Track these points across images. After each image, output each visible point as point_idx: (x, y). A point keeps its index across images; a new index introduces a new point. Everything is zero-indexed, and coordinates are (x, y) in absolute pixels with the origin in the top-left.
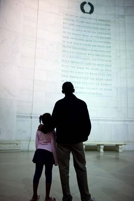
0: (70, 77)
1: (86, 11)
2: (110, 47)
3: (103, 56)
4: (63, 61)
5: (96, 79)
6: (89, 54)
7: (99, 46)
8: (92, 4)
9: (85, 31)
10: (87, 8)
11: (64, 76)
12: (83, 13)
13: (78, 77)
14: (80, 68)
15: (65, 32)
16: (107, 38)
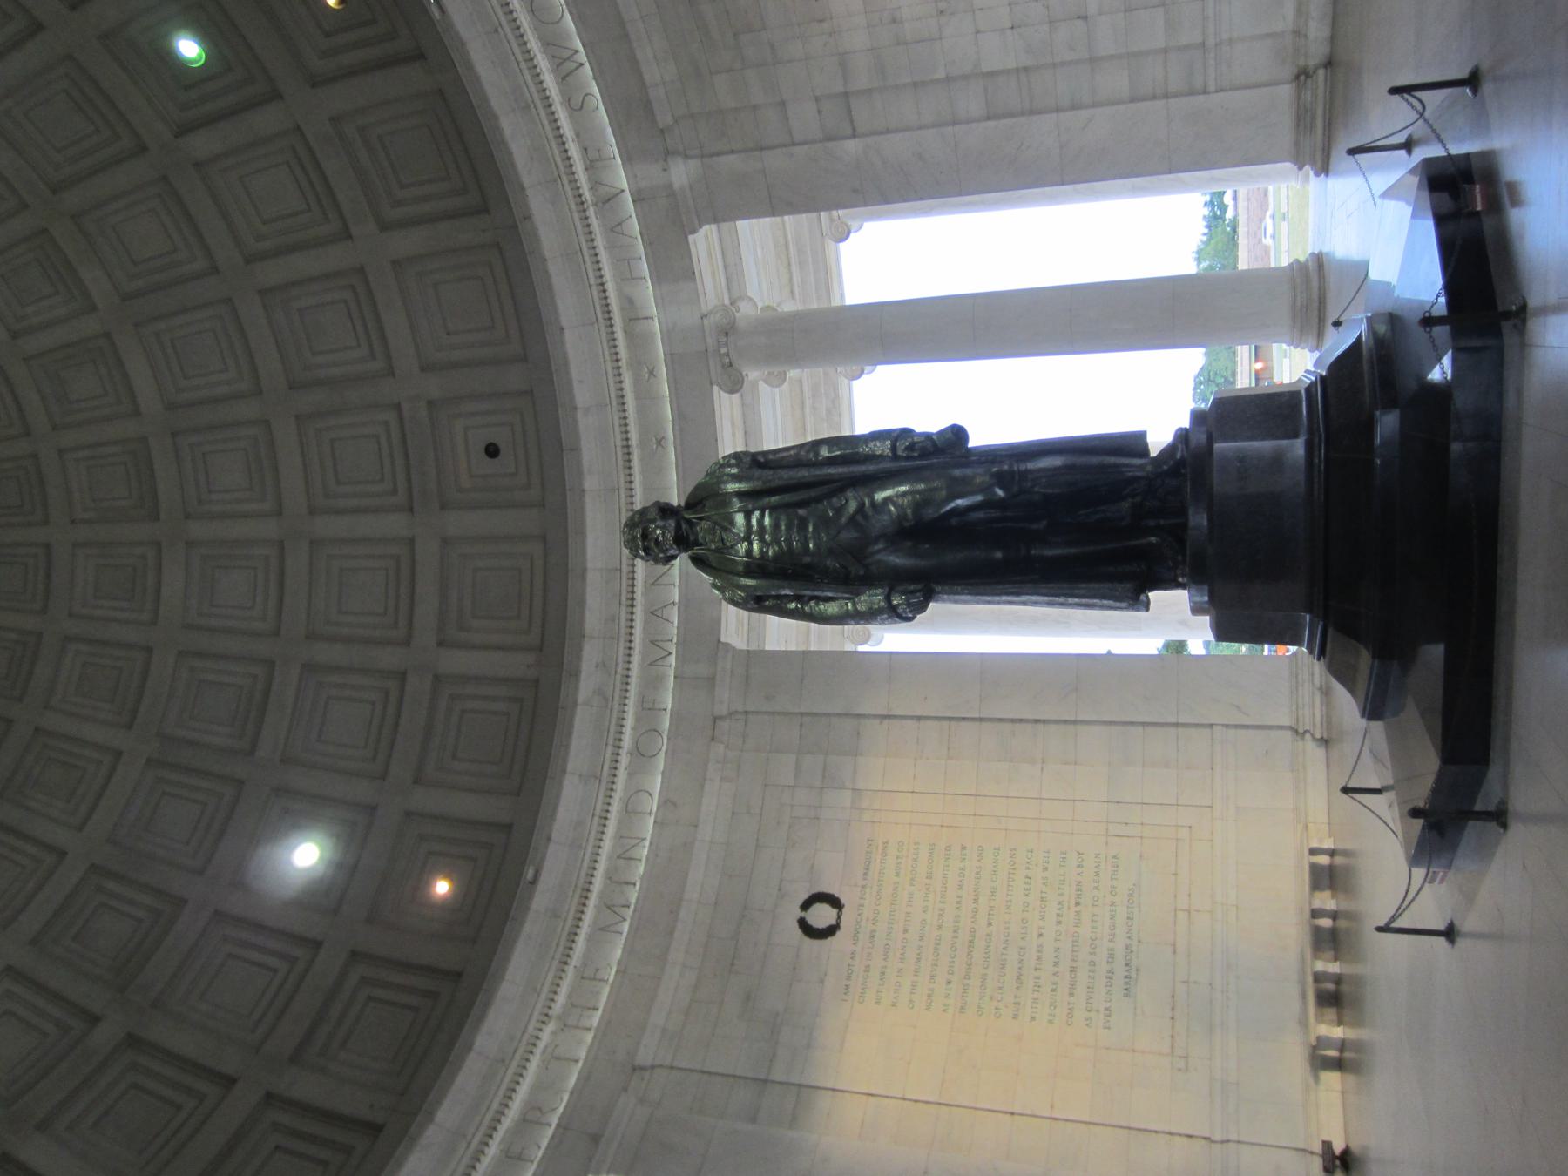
0: (1071, 994)
1: (833, 922)
2: (964, 848)
3: (995, 873)
4: (1015, 1017)
5: (1077, 904)
6: (990, 924)
7: (960, 888)
8: (805, 896)
9: (906, 931)
10: (822, 916)
11: (1070, 1014)
12: (838, 934)
13: (1073, 970)
14: (1039, 958)
15: (911, 1001)
16: (931, 855)
